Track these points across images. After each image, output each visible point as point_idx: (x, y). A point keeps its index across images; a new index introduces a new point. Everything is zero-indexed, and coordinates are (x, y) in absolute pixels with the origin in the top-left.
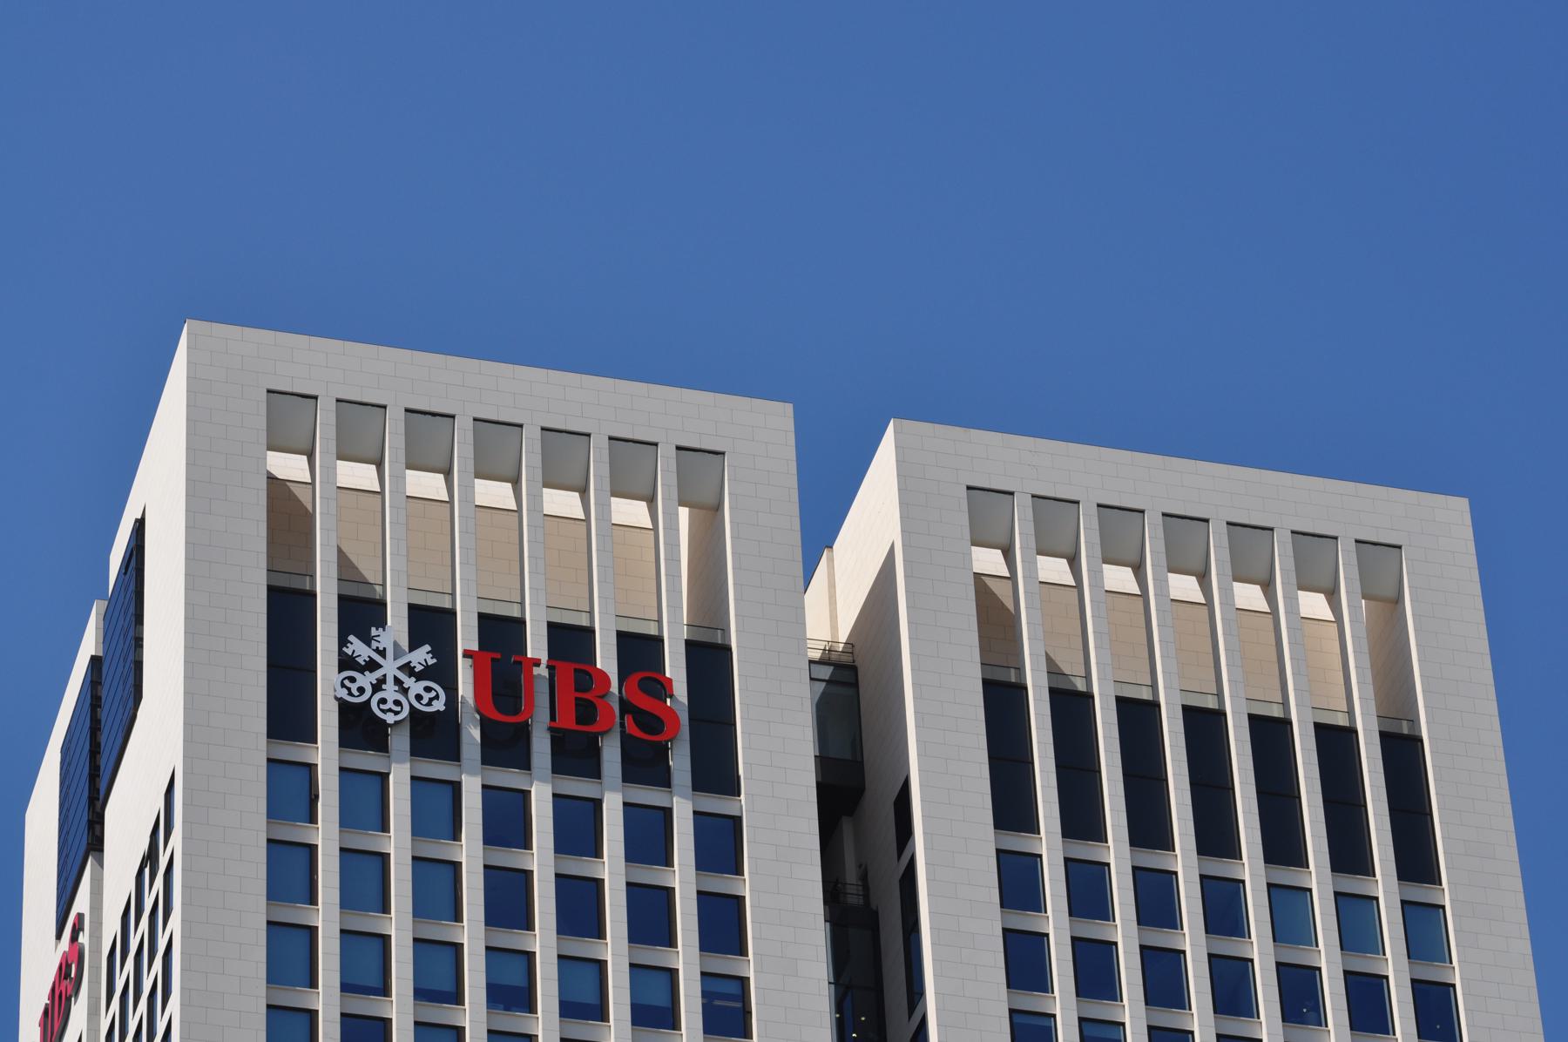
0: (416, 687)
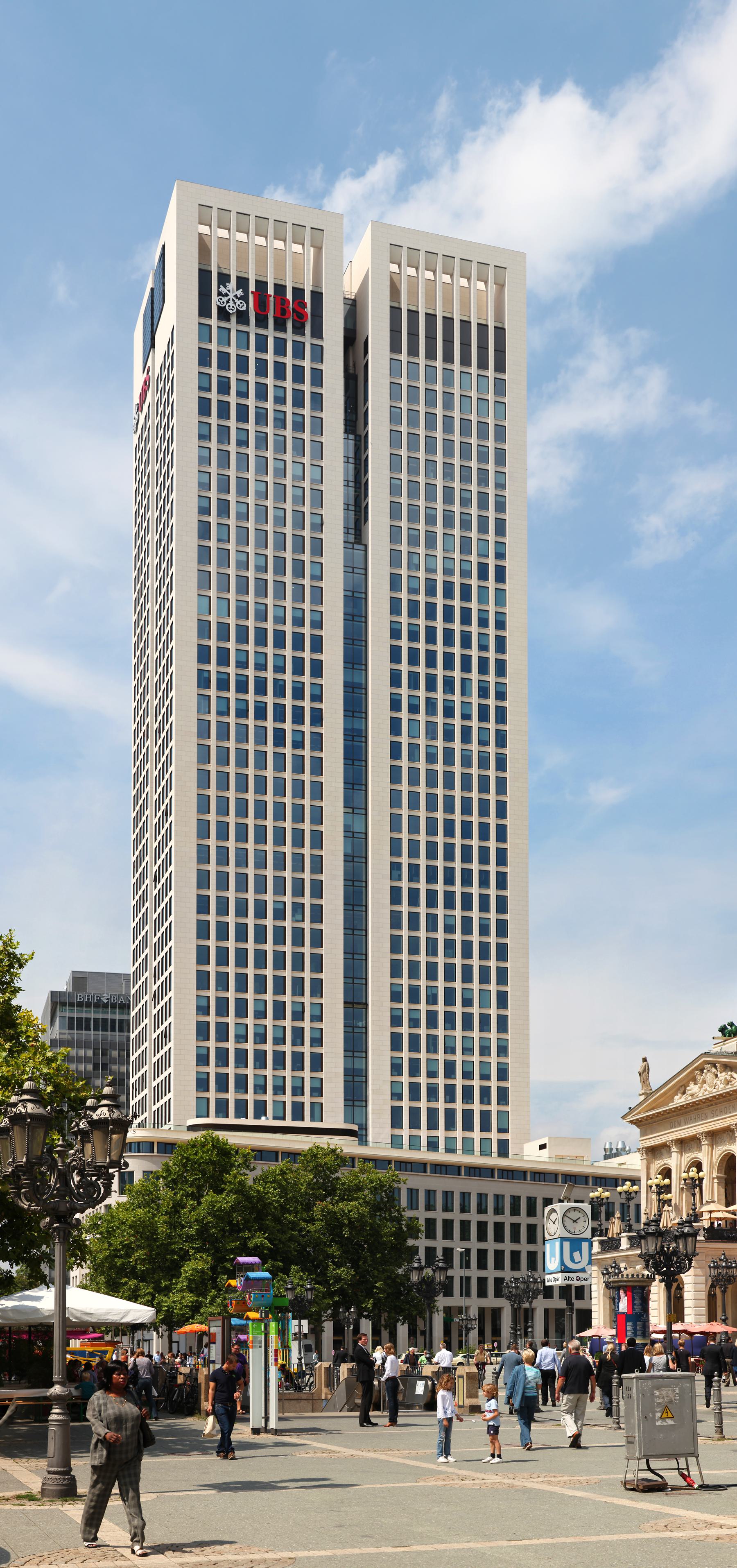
0: (238, 302)
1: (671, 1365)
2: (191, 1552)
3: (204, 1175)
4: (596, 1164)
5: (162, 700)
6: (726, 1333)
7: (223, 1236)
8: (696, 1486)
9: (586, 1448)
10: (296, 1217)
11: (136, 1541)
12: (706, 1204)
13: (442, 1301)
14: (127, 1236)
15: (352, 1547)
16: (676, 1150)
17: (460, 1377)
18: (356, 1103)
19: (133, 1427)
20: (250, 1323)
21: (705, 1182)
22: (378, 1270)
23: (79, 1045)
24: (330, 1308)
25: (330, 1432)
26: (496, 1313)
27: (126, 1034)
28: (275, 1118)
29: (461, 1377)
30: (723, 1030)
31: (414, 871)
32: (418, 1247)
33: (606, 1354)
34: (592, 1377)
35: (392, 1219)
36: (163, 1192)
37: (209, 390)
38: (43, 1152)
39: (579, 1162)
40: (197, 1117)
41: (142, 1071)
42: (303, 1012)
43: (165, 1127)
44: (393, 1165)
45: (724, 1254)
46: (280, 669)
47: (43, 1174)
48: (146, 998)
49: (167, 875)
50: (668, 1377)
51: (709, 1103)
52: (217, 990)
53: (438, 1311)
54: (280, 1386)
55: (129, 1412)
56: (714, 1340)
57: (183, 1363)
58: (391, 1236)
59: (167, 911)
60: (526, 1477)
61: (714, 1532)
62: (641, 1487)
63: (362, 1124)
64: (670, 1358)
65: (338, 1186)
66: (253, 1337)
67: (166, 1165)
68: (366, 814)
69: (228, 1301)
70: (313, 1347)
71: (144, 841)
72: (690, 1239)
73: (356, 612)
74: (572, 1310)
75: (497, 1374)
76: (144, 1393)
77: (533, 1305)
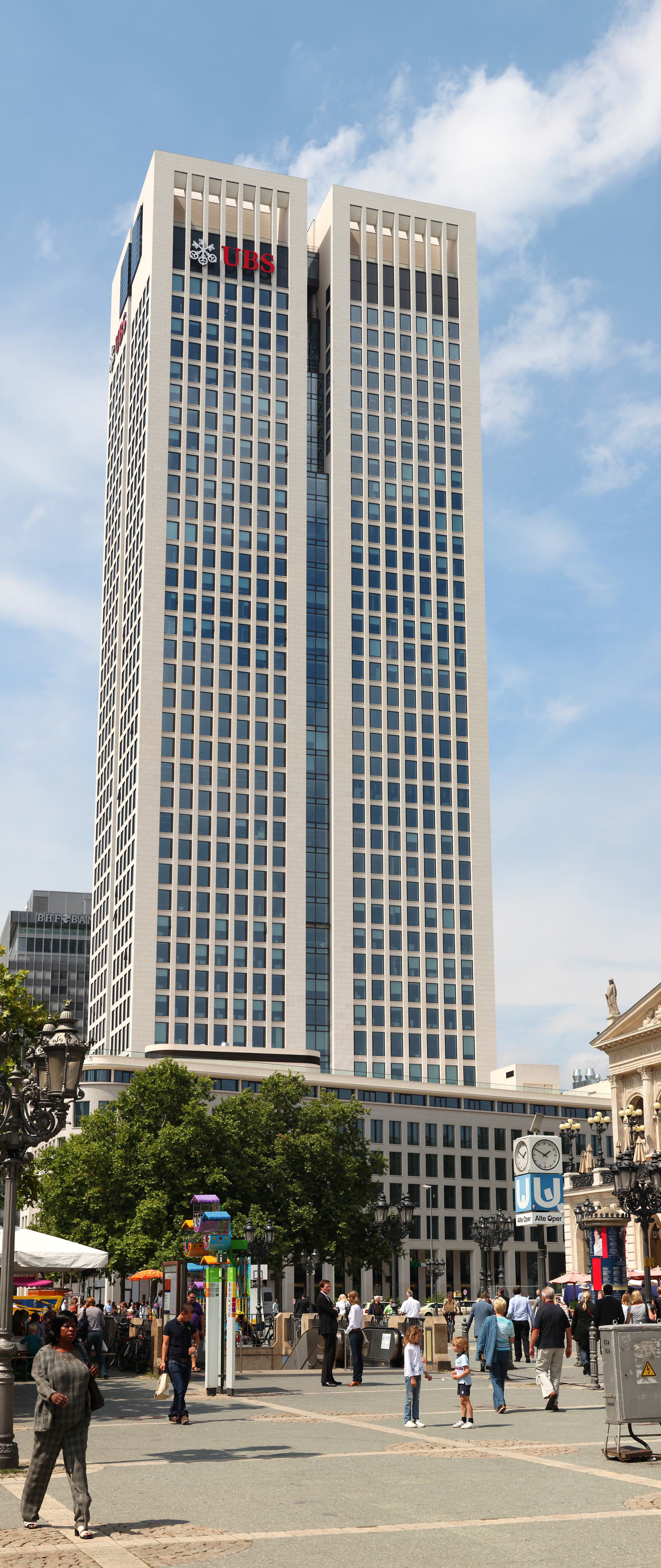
3: (161, 1106)
4: (565, 1093)
7: (180, 1172)
10: (256, 1150)
14: (80, 1172)
18: (319, 1028)
19: (80, 1386)
20: (207, 1268)
24: (290, 1251)
26: (465, 1256)
32: (382, 1184)
33: (582, 1303)
35: (356, 1153)
36: (119, 1123)
39: (547, 1091)
44: (356, 1095)
53: (404, 1254)
54: (237, 1340)
55: (77, 1370)
57: (136, 1314)
58: (355, 1172)
63: (325, 1051)
65: (299, 1117)
69: (184, 1244)
70: (273, 1295)
74: (544, 1253)
75: (467, 1326)
76: (93, 1347)
77: (504, 1249)
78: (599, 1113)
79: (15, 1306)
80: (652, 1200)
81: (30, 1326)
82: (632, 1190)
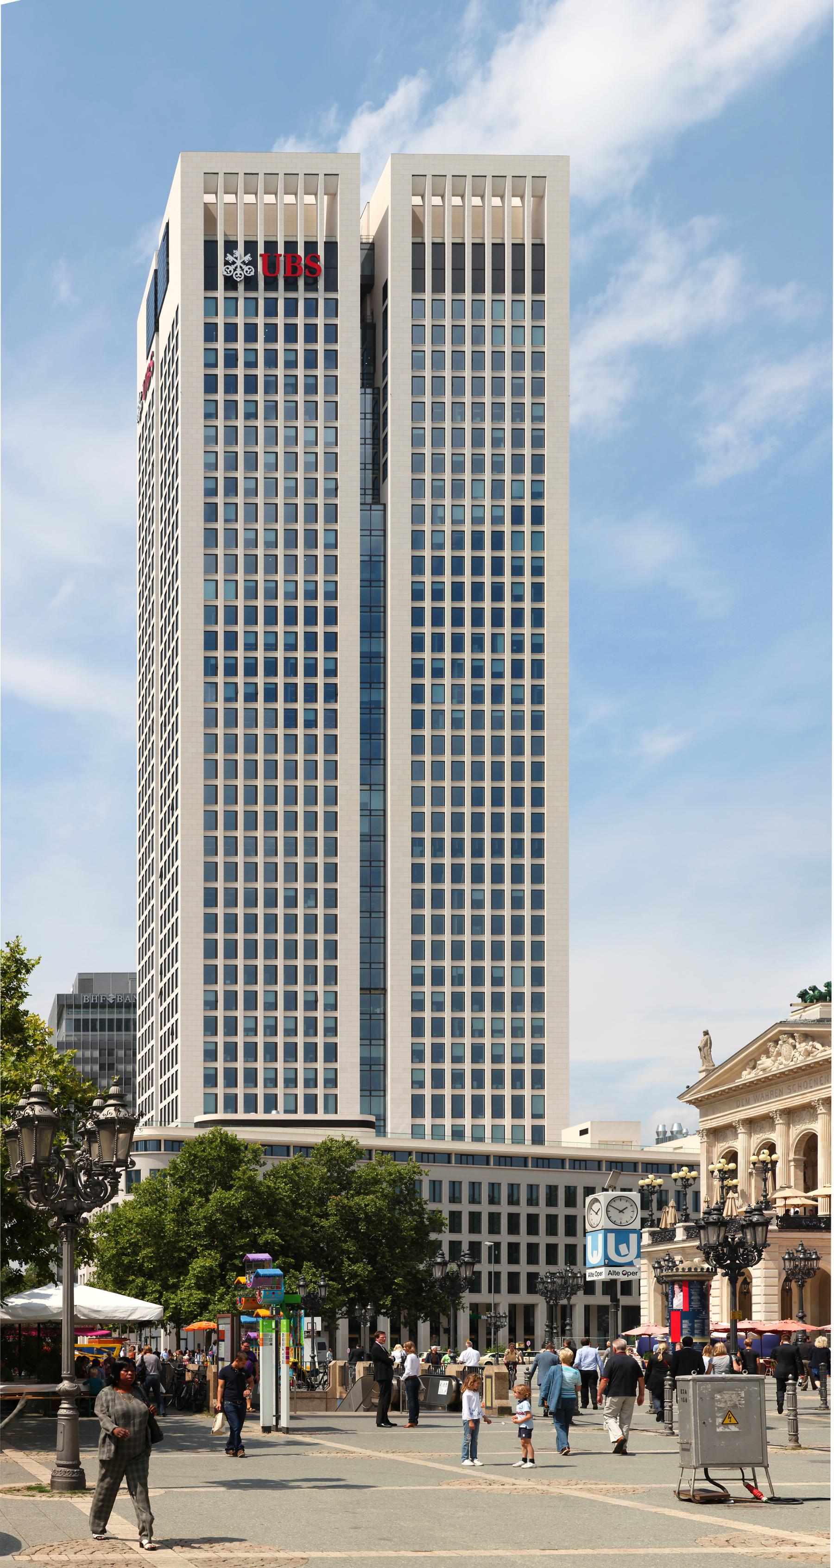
0: (246, 268)
1: (736, 1367)
2: (199, 1548)
3: (212, 1172)
4: (646, 1149)
5: (167, 693)
6: (804, 1331)
7: (232, 1233)
8: (764, 1499)
9: (633, 1454)
10: (308, 1212)
11: (145, 1535)
12: (779, 1190)
13: (467, 1298)
14: (134, 1234)
15: (369, 1549)
16: (743, 1131)
17: (487, 1377)
18: (373, 1093)
19: (141, 1422)
20: (260, 1320)
21: (779, 1167)
22: (397, 1266)
23: (85, 1046)
24: (345, 1305)
25: (345, 1432)
26: (529, 1310)
27: (132, 1033)
28: (286, 1112)
29: (490, 1377)
30: (803, 995)
31: (438, 847)
32: (441, 1242)
33: (657, 1354)
34: (640, 1379)
35: (413, 1213)
36: (170, 1189)
37: (216, 365)
38: (50, 1153)
39: (625, 1148)
40: (205, 1113)
41: (149, 1069)
42: (316, 1001)
43: (172, 1125)
44: (414, 1157)
45: (802, 1245)
46: (291, 647)
47: (51, 1175)
48: (153, 995)
49: (173, 870)
50: (732, 1380)
51: (785, 1078)
52: (225, 983)
53: (463, 1308)
54: (292, 1384)
55: (137, 1408)
56: (789, 1339)
57: (191, 1360)
58: (411, 1230)
59: (174, 906)
60: (563, 1483)
61: (787, 1549)
62: (698, 1498)
63: (380, 1115)
64: (734, 1359)
65: (353, 1180)
66: (264, 1335)
67: (174, 1163)
68: (385, 790)
69: (238, 1298)
70: (327, 1345)
71: (149, 838)
72: (760, 1229)
73: (374, 577)
74: (617, 1306)
75: (530, 1375)
76: (151, 1389)
77: (572, 1302)
78: (685, 1168)
79: (76, 1353)
80: (743, 1255)
81: (92, 1370)
82: (720, 1244)
